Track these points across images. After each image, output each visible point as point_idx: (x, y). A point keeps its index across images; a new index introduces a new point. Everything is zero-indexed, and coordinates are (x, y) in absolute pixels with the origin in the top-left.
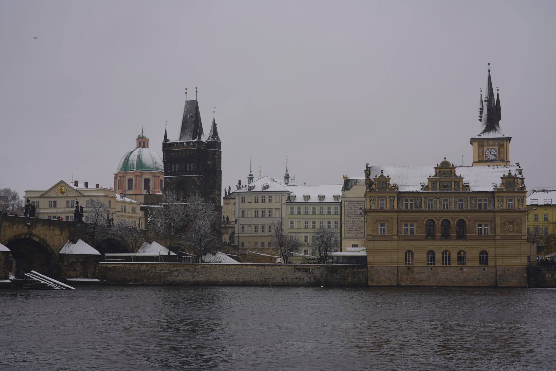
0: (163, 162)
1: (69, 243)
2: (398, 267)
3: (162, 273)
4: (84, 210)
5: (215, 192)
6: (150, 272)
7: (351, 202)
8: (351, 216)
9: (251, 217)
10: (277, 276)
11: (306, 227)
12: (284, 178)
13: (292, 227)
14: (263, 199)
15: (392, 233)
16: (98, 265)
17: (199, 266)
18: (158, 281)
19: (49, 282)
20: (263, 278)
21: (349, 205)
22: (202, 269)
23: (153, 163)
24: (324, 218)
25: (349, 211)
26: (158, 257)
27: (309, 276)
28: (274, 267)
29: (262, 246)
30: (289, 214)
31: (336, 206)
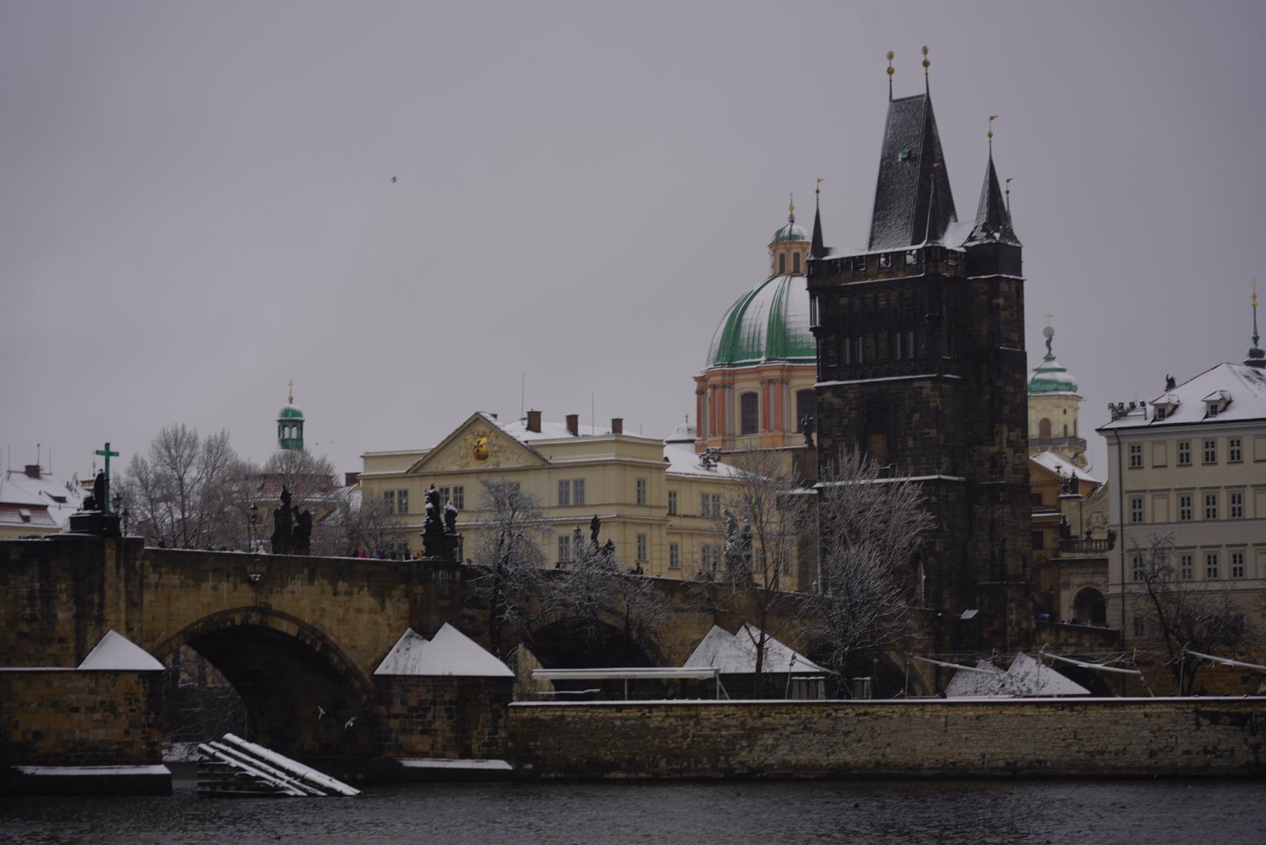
0: (811, 329)
3: (722, 737)
4: (461, 521)
6: (680, 734)
9: (1164, 520)
10: (1130, 744)
14: (1210, 450)
16: (507, 712)
17: (849, 710)
18: (708, 766)
19: (272, 770)
22: (859, 721)
26: (713, 680)
27: (1251, 740)
28: (1122, 711)
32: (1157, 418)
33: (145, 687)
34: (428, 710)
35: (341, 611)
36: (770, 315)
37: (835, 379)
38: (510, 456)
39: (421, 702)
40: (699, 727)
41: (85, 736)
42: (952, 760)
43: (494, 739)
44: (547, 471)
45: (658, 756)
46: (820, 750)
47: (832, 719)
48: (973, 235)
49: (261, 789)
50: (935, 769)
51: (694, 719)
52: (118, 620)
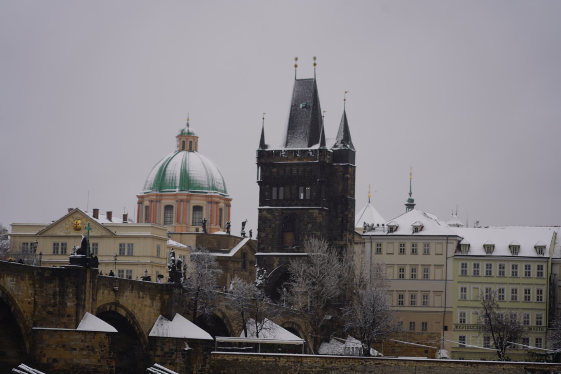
0: (258, 182)
1: (161, 319)
3: (313, 371)
5: (347, 235)
12: (405, 207)
13: (464, 298)
16: (210, 356)
17: (372, 362)
22: (376, 367)
23: (208, 178)
24: (519, 284)
28: (493, 367)
29: (411, 329)
30: (459, 276)
31: (540, 264)
32: (389, 232)
33: (109, 340)
34: (174, 354)
35: (140, 306)
37: (269, 206)
39: (170, 350)
40: (302, 367)
41: (78, 362)
43: (204, 368)
47: (364, 366)
51: (300, 363)
52: (89, 308)
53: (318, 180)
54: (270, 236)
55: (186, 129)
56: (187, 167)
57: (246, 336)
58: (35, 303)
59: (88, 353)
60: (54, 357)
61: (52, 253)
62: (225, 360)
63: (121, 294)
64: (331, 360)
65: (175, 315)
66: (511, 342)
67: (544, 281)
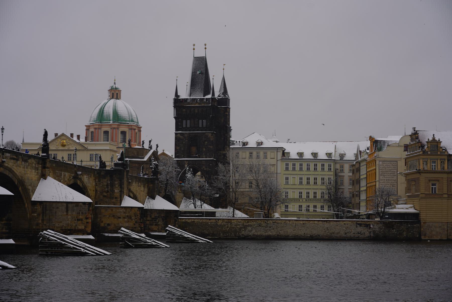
0: (174, 117)
1: (148, 198)
2: (447, 222)
3: (237, 228)
7: (385, 162)
8: (385, 175)
10: (341, 231)
11: (301, 183)
13: (287, 183)
15: (443, 192)
16: (178, 220)
18: (234, 235)
20: (328, 233)
21: (383, 164)
22: (273, 224)
23: (129, 115)
24: (318, 175)
25: (383, 170)
27: (369, 230)
28: (338, 223)
30: (284, 171)
35: (139, 191)
36: (113, 109)
37: (181, 131)
38: (73, 146)
42: (296, 235)
44: (86, 151)
45: (220, 232)
46: (263, 231)
48: (220, 95)
49: (189, 241)
50: (292, 237)
51: (230, 223)
53: (211, 116)
54: (182, 149)
55: (114, 86)
56: (117, 109)
57: (195, 208)
58: (96, 190)
59: (128, 220)
60: (108, 222)
61: (89, 160)
62: (187, 222)
63: (132, 184)
64: (248, 221)
65: (156, 196)
66: (344, 209)
67: (332, 173)
